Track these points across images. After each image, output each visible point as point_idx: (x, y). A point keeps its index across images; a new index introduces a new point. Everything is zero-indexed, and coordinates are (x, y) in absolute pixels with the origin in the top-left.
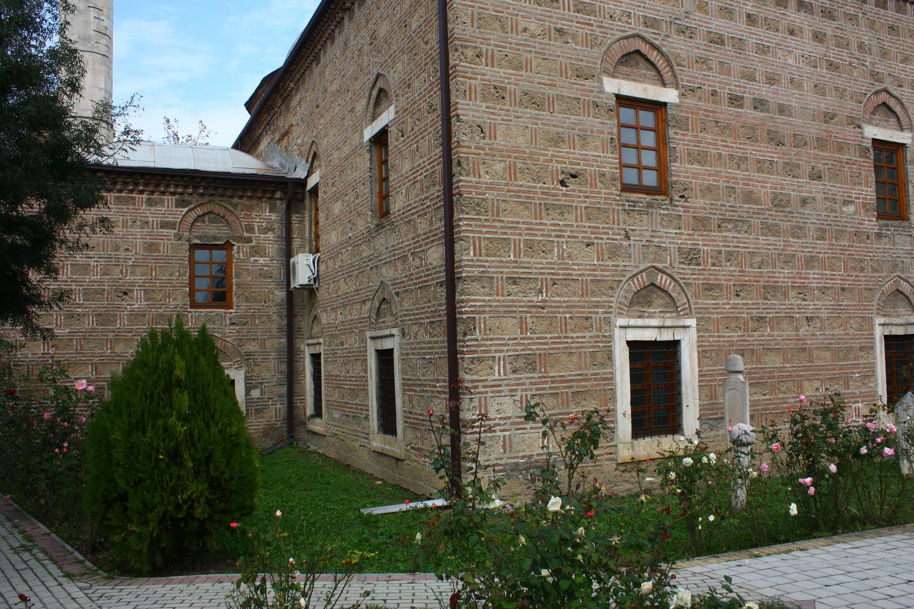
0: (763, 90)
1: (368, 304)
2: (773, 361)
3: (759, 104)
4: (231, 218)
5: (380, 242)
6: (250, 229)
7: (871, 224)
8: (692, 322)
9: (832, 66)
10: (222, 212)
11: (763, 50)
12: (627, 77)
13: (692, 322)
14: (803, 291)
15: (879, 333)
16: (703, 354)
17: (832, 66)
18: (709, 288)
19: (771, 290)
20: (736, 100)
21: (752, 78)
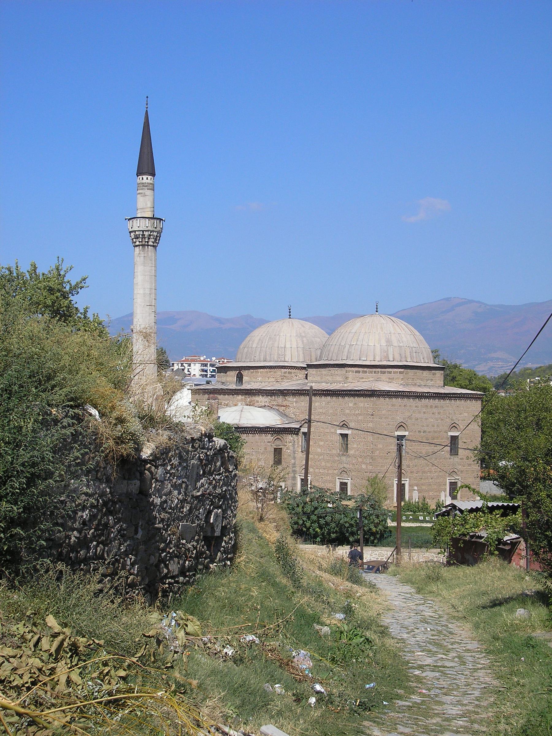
0: (425, 428)
1: (337, 471)
2: (424, 487)
3: (424, 432)
4: (282, 439)
5: (344, 458)
6: (286, 443)
7: (448, 456)
8: (408, 479)
9: (442, 420)
10: (280, 437)
11: (426, 419)
12: (399, 431)
13: (408, 479)
14: (430, 472)
15: (448, 481)
16: (410, 486)
17: (442, 420)
18: (411, 472)
19: (424, 472)
20: (420, 432)
21: (423, 426)
